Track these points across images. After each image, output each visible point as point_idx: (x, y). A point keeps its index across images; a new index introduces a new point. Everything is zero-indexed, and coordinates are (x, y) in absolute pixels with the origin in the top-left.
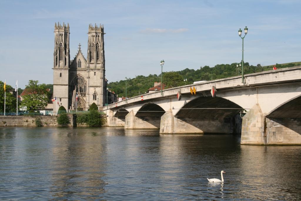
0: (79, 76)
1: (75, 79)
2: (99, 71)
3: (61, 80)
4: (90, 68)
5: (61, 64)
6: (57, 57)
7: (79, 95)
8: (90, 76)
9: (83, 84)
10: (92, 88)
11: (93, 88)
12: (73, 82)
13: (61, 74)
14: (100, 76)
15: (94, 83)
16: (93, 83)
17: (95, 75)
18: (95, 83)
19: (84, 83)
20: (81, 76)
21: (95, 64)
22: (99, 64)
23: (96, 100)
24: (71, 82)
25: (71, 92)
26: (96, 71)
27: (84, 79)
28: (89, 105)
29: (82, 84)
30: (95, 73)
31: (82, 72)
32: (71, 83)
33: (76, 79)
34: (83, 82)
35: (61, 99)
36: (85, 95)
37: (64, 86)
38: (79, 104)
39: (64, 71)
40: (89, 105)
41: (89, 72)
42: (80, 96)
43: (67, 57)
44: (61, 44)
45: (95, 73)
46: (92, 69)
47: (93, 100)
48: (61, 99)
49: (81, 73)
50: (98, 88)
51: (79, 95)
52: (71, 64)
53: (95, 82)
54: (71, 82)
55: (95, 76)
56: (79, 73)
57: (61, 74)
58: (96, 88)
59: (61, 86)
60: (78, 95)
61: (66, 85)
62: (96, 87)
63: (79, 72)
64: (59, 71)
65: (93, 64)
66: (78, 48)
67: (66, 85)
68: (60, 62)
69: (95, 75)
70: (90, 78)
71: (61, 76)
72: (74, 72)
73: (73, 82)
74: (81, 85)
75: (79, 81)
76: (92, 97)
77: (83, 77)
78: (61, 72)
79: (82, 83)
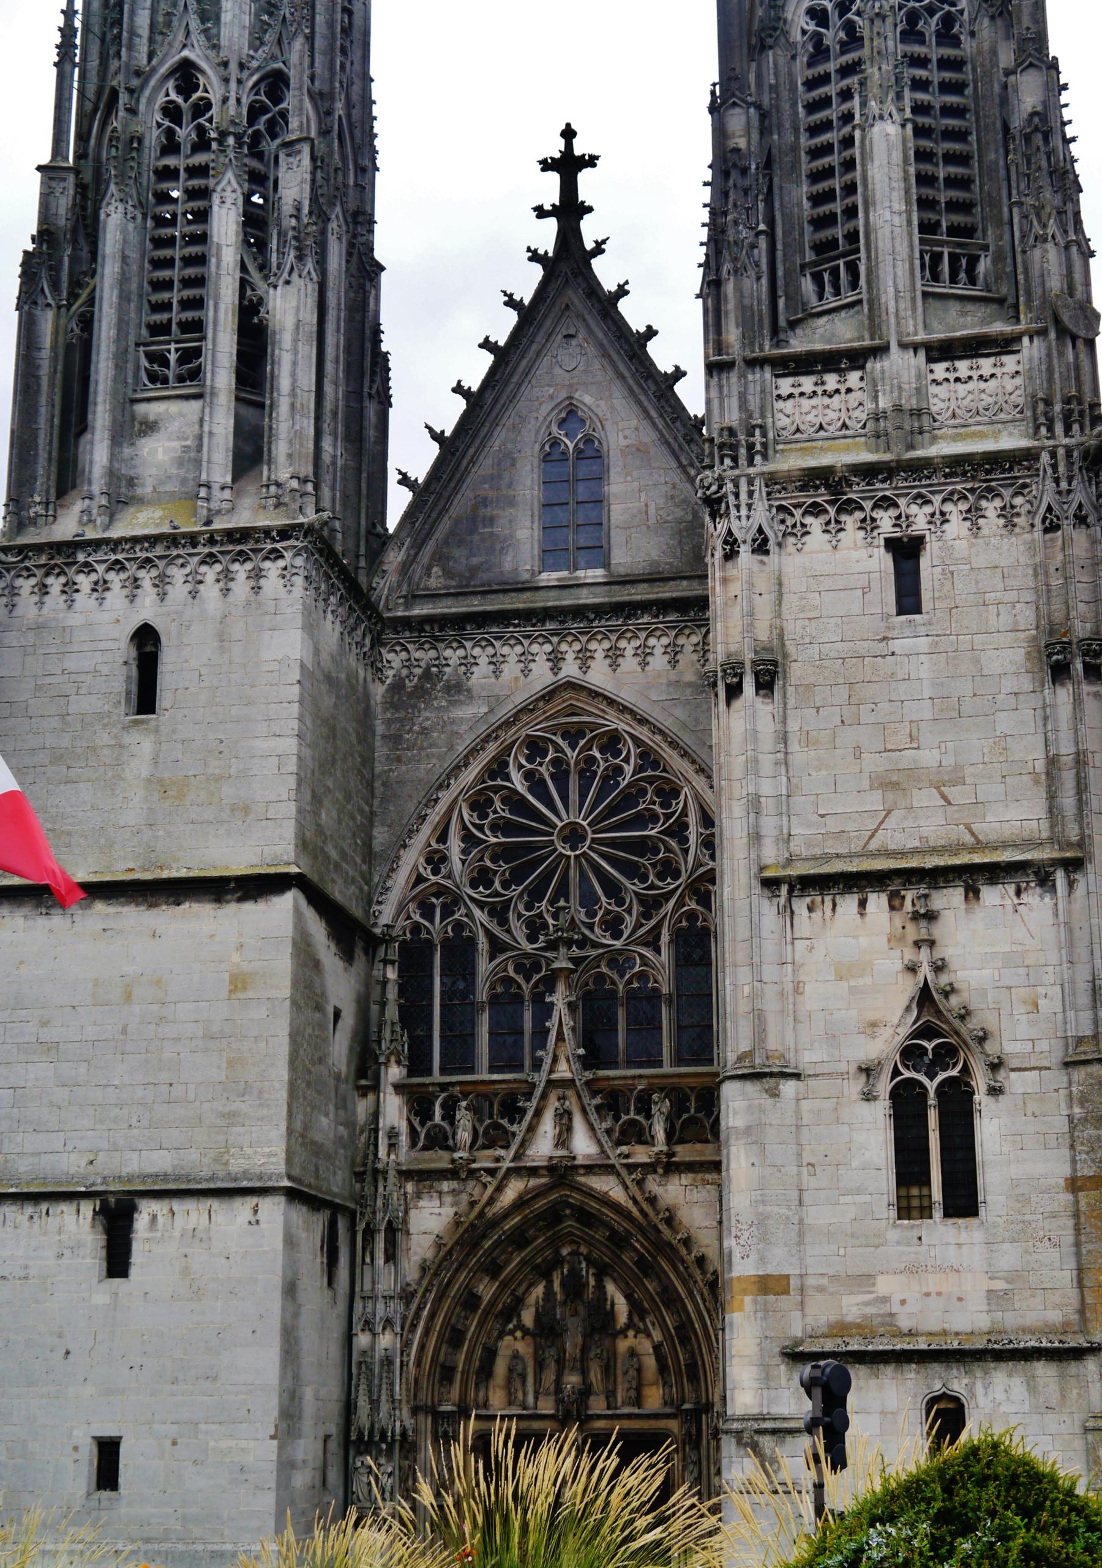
0: (573, 735)
1: (480, 805)
2: (991, 508)
3: (139, 767)
4: (790, 462)
5: (157, 454)
6: (87, 322)
7: (563, 1138)
8: (793, 629)
9: (650, 905)
10: (848, 904)
11: (877, 902)
12: (436, 860)
13: (146, 639)
14: (1027, 617)
15: (887, 784)
16: (875, 801)
17: (908, 598)
18: (926, 798)
19: (669, 870)
20: (612, 742)
21: (874, 366)
22: (986, 365)
23: (963, 1201)
24: (412, 858)
25: (394, 1073)
26: (920, 518)
27: (669, 793)
28: (794, 1356)
29: (632, 886)
30: (906, 552)
31: (614, 656)
32: (401, 878)
33: (499, 809)
34: (642, 846)
35: (116, 1217)
36: (697, 1118)
37: (198, 918)
38: (572, 1344)
39: (210, 590)
40: (794, 1356)
41: (761, 547)
42: (583, 1145)
43: (289, 307)
44: (186, 75)
45: (906, 552)
46: (830, 491)
47: (905, 1210)
48: (116, 1217)
49: (599, 676)
50: (991, 895)
51: (563, 1138)
52: (409, 516)
53: (928, 757)
54: (412, 858)
55: (912, 639)
56: (570, 669)
57: (146, 639)
58: (949, 899)
59: (131, 917)
60: (548, 1127)
61: (256, 886)
62: (936, 877)
63: (570, 651)
64: (101, 587)
65: (857, 358)
66: (541, 212)
67: (256, 886)
68: (149, 427)
69: (908, 598)
70: (797, 671)
71: (146, 699)
72: (453, 655)
73: (436, 860)
74: (613, 926)
75: (574, 835)
76: (872, 1135)
77: (648, 758)
78: (147, 609)
79: (632, 871)
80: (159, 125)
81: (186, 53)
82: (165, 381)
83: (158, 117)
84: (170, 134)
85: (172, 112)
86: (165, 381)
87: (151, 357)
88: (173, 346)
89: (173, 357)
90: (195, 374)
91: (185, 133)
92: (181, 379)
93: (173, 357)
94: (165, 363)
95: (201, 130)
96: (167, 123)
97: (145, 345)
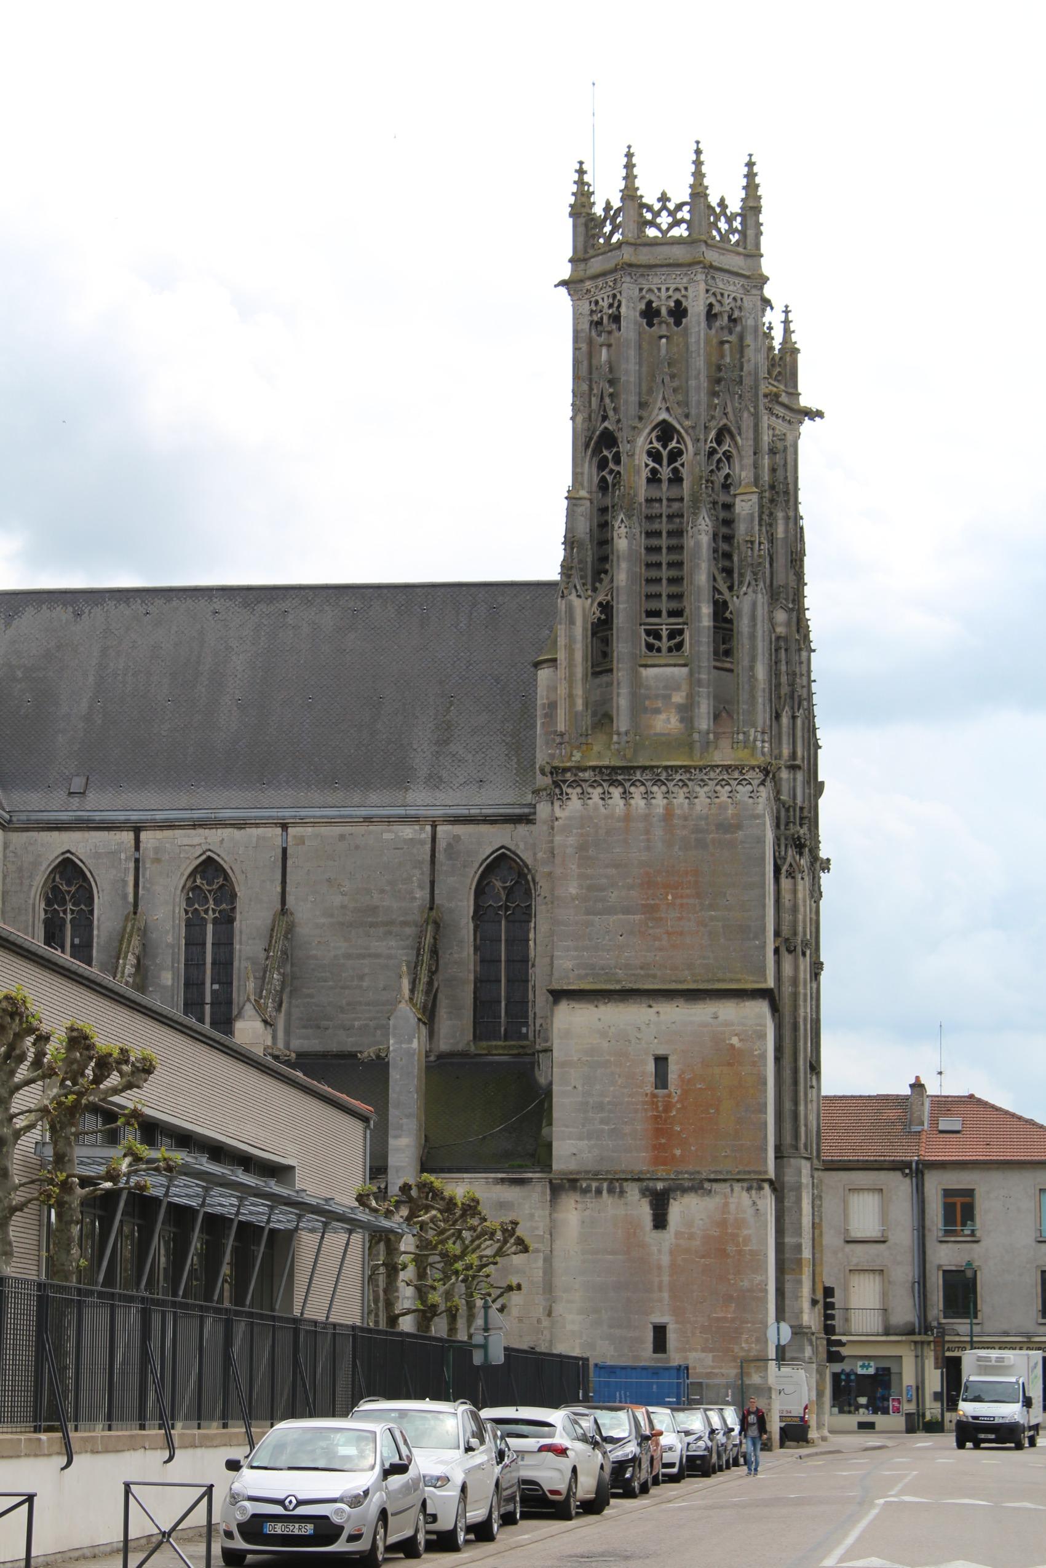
80: (647, 465)
81: (664, 416)
82: (659, 650)
83: (645, 458)
84: (654, 471)
85: (655, 456)
86: (659, 650)
87: (648, 633)
88: (664, 627)
89: (664, 634)
90: (679, 646)
91: (665, 472)
92: (670, 650)
93: (664, 634)
94: (658, 637)
95: (676, 471)
96: (652, 464)
97: (645, 624)
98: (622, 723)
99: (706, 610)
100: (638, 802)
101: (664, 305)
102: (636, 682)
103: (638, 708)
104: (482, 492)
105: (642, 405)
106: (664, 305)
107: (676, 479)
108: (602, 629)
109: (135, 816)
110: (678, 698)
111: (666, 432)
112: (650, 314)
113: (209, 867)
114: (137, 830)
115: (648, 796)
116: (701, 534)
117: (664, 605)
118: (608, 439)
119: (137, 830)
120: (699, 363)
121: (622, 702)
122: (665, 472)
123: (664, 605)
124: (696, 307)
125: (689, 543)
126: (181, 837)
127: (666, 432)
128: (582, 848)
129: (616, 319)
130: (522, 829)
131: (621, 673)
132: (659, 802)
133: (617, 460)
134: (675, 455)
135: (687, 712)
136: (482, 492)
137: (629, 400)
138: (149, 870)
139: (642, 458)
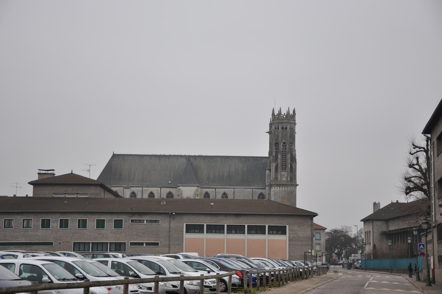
98: (279, 179)
99: (289, 165)
100: (281, 189)
101: (284, 127)
102: (281, 174)
103: (281, 177)
104: (259, 147)
105: (282, 140)
106: (284, 127)
107: (286, 149)
108: (276, 168)
109: (215, 187)
110: (286, 176)
111: (284, 143)
112: (283, 128)
113: (225, 193)
114: (216, 189)
115: (282, 188)
116: (289, 156)
117: (284, 164)
118: (277, 143)
119: (216, 189)
120: (289, 135)
121: (279, 176)
122: (284, 148)
123: (284, 164)
124: (288, 128)
125: (287, 157)
126: (221, 190)
127: (284, 143)
128: (274, 194)
129: (278, 128)
130: (264, 190)
131: (279, 173)
132: (284, 189)
133: (278, 146)
134: (285, 146)
135: (287, 178)
136: (259, 147)
137: (280, 139)
138: (217, 194)
139: (281, 146)
